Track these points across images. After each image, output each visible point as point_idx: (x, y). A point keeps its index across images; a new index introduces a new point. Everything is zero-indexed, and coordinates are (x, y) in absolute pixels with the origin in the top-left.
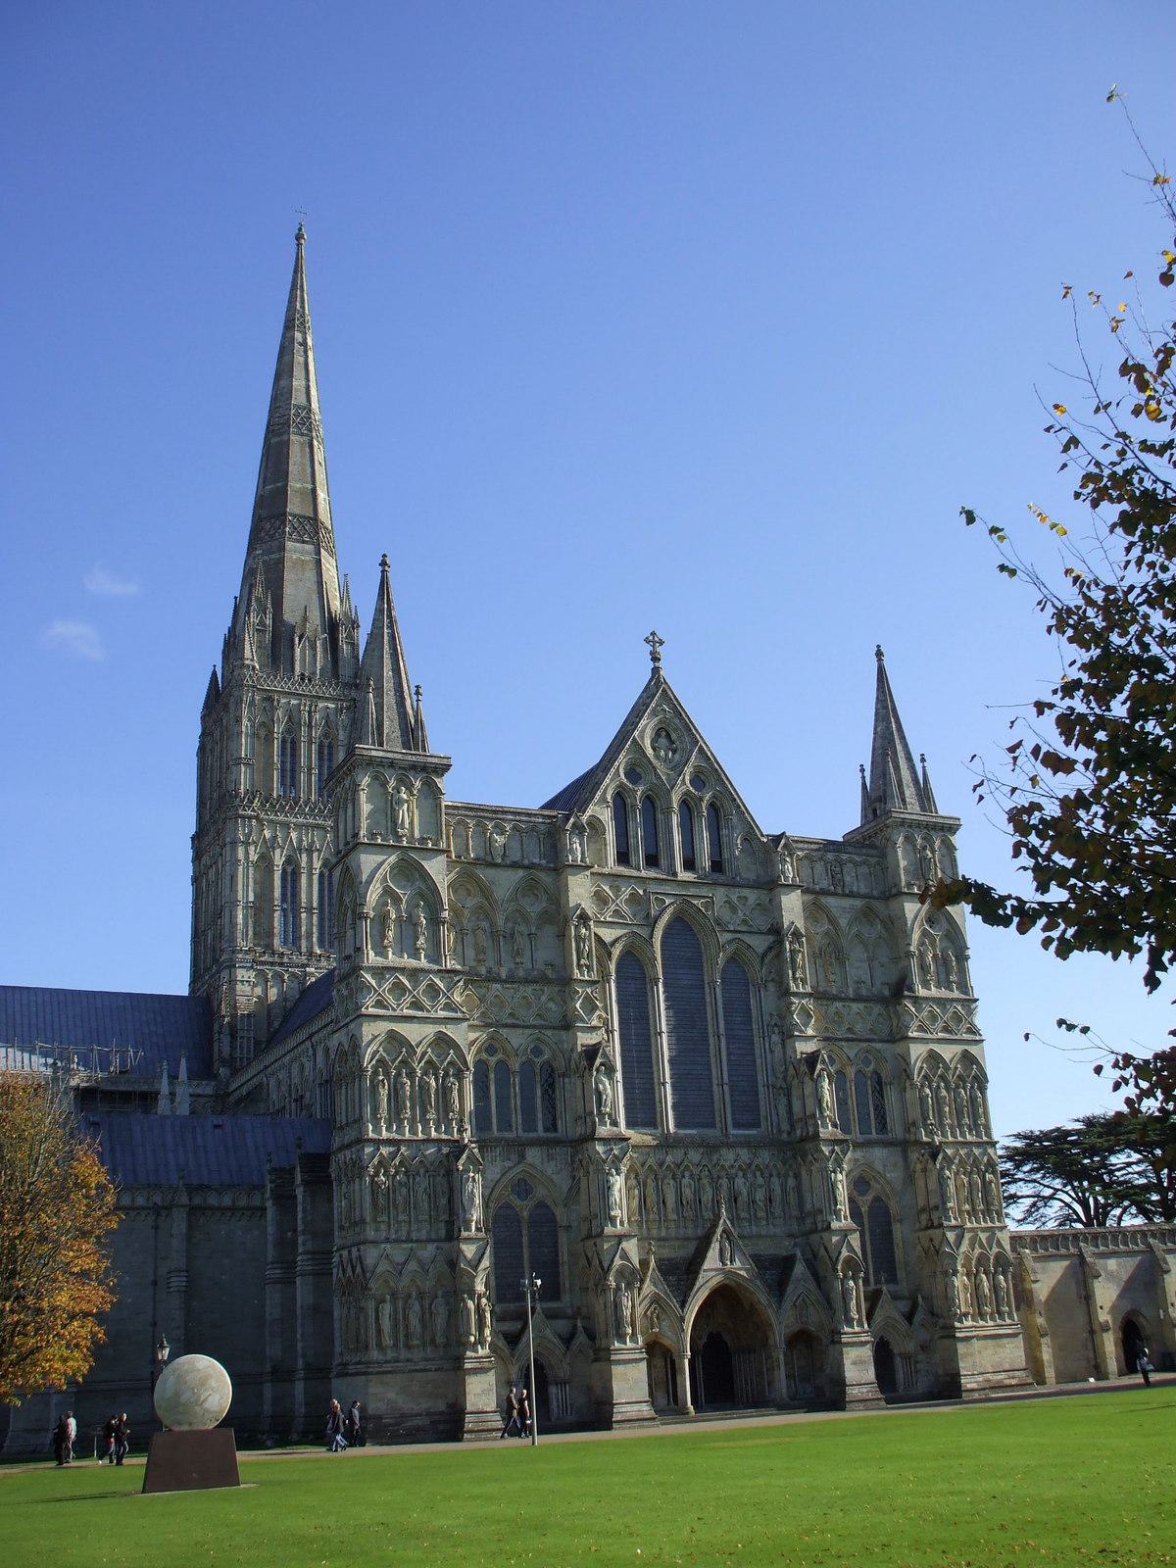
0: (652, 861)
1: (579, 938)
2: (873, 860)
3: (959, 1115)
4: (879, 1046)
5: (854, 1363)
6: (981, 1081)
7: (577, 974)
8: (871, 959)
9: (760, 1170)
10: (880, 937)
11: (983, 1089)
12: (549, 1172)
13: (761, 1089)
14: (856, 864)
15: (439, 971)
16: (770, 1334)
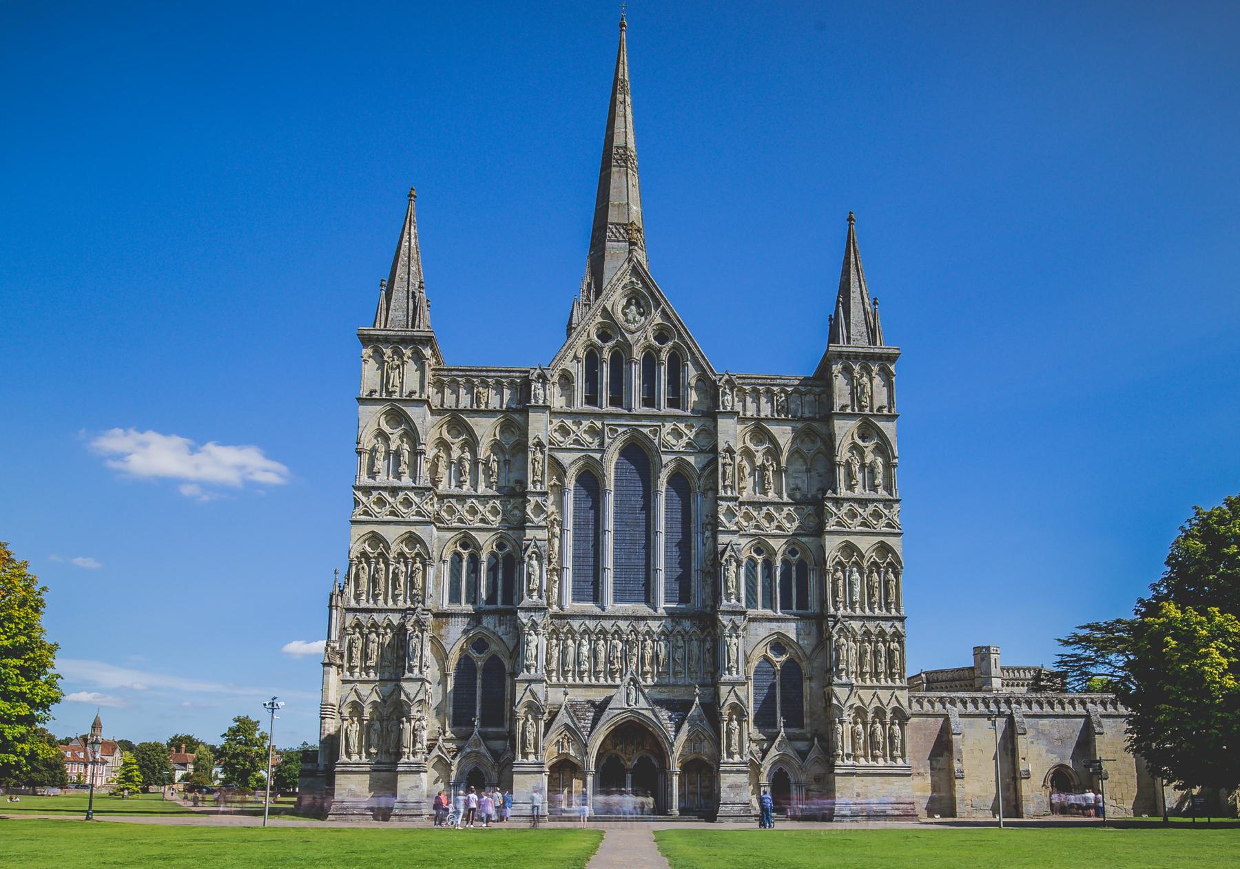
0: (616, 401)
1: (534, 460)
2: (817, 390)
3: (871, 596)
4: (804, 539)
5: (729, 787)
6: (895, 567)
7: (530, 487)
8: (808, 471)
9: (682, 636)
10: (819, 453)
11: (897, 575)
12: (500, 634)
13: (693, 572)
14: (801, 394)
15: (414, 488)
16: (667, 760)
